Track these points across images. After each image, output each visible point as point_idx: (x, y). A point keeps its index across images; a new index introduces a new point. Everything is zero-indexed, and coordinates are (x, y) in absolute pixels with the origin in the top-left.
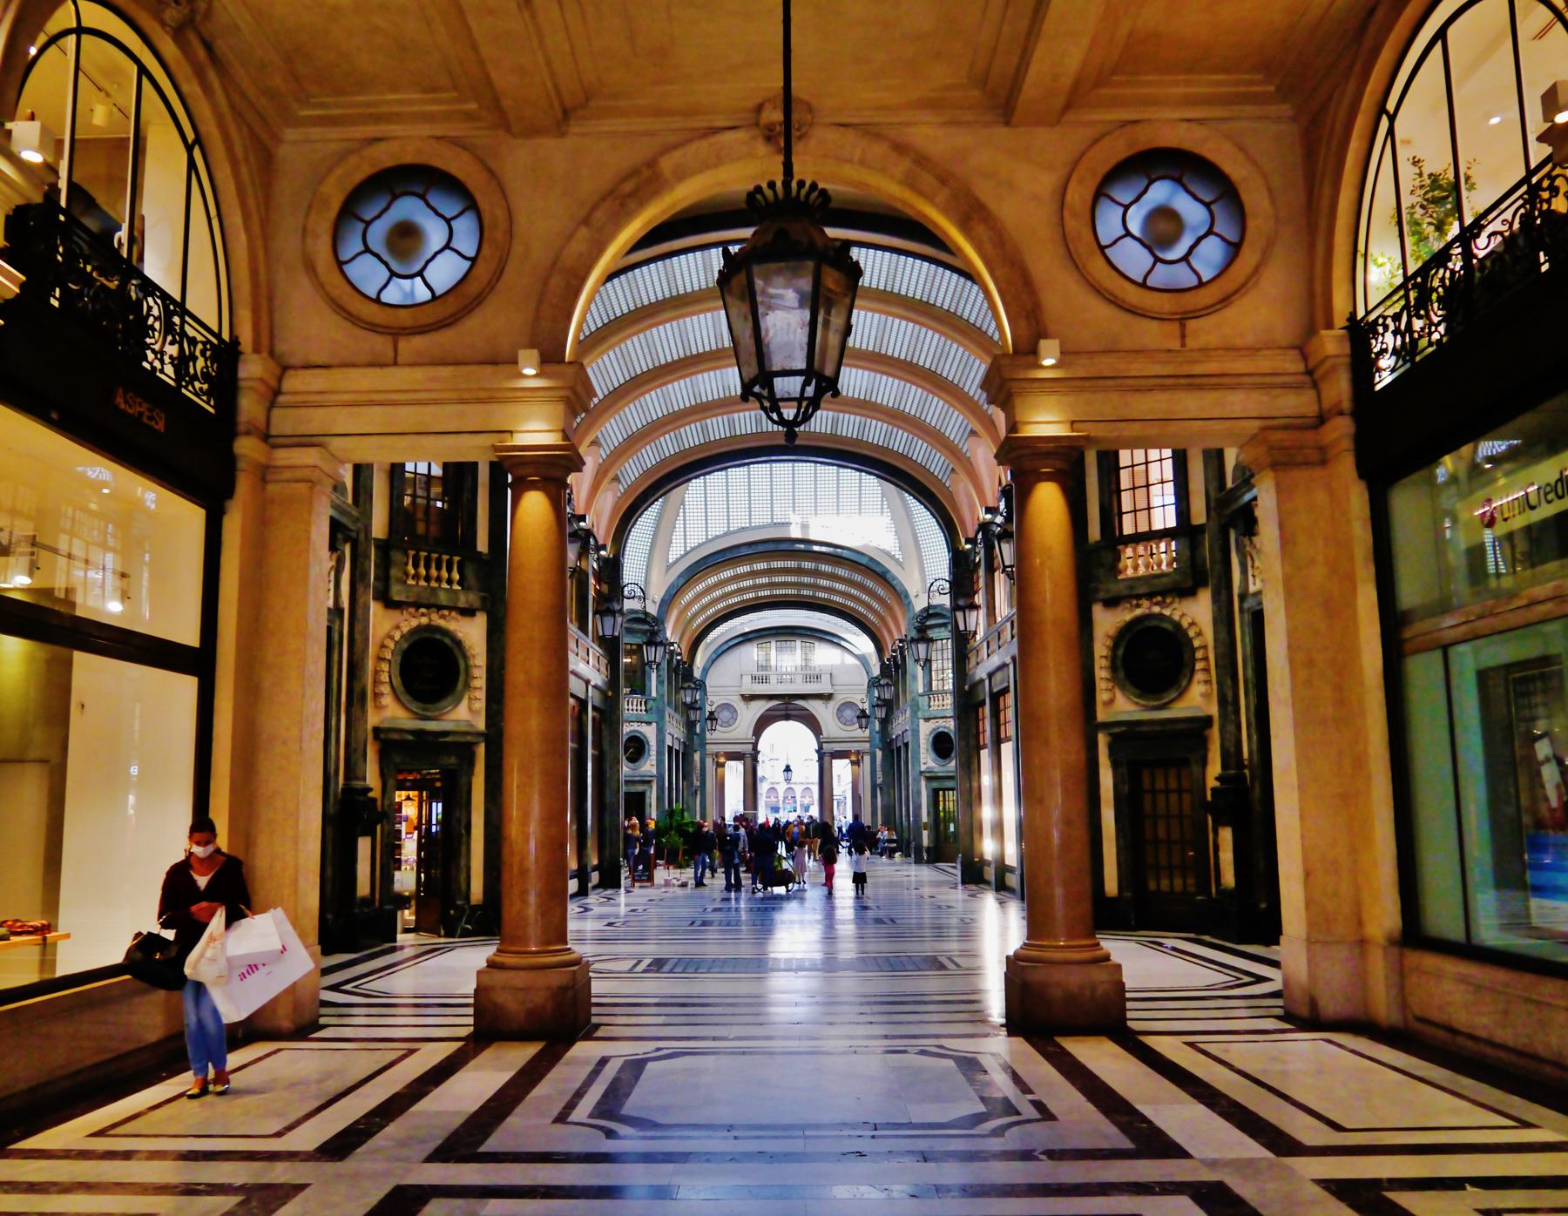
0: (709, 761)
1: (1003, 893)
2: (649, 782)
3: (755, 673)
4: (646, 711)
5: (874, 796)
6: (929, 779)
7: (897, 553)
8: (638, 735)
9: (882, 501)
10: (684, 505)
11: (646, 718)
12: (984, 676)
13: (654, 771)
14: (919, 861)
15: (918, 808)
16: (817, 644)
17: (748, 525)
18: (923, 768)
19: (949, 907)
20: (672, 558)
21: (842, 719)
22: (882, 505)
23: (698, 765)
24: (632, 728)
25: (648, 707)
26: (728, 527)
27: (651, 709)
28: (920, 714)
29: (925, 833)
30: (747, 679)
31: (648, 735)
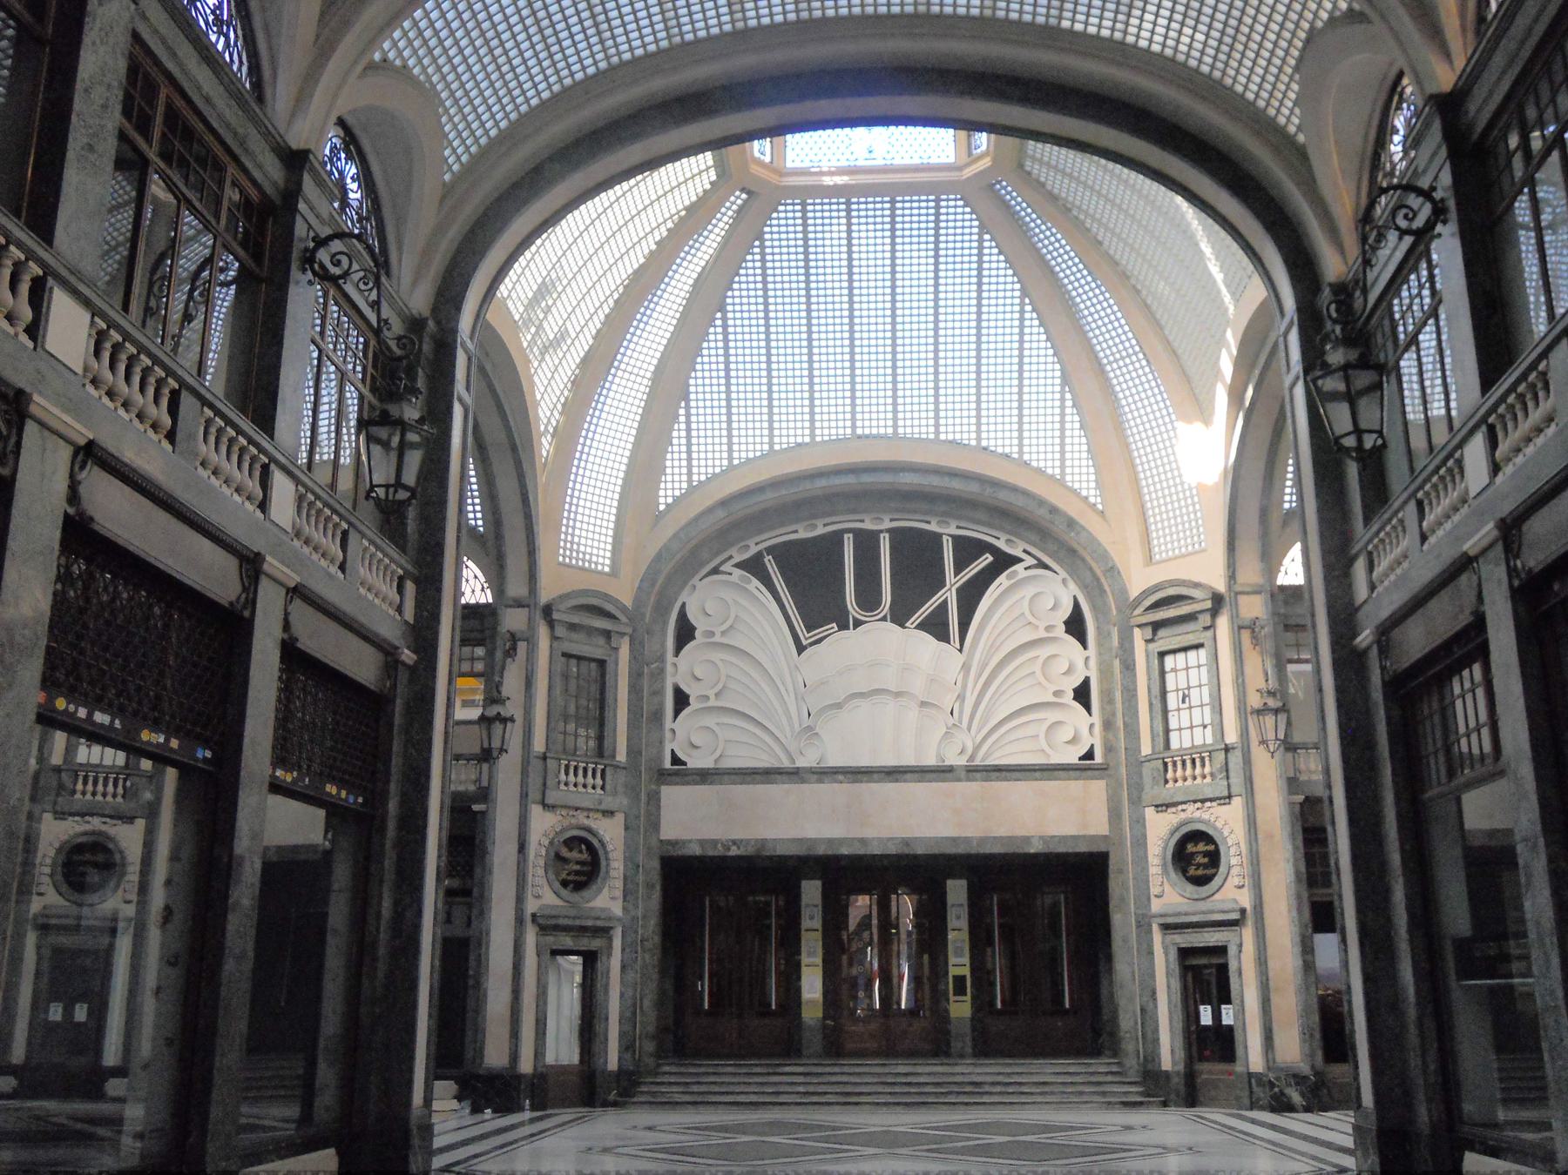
4: (603, 788)
7: (1092, 492)
9: (1062, 392)
10: (688, 401)
17: (807, 439)
18: (1156, 906)
20: (665, 497)
22: (1063, 400)
26: (771, 444)
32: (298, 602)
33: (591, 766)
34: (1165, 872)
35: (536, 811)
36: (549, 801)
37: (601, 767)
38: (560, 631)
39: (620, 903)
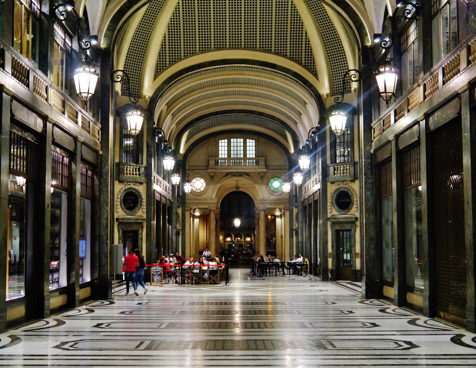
1: (381, 300)
2: (141, 223)
4: (139, 174)
5: (291, 237)
8: (134, 191)
12: (391, 137)
13: (145, 216)
14: (325, 279)
15: (325, 243)
18: (329, 215)
19: (351, 312)
23: (181, 216)
24: (129, 186)
29: (330, 260)
32: (14, 101)
33: (135, 167)
34: (332, 204)
35: (116, 183)
36: (121, 180)
37: (138, 167)
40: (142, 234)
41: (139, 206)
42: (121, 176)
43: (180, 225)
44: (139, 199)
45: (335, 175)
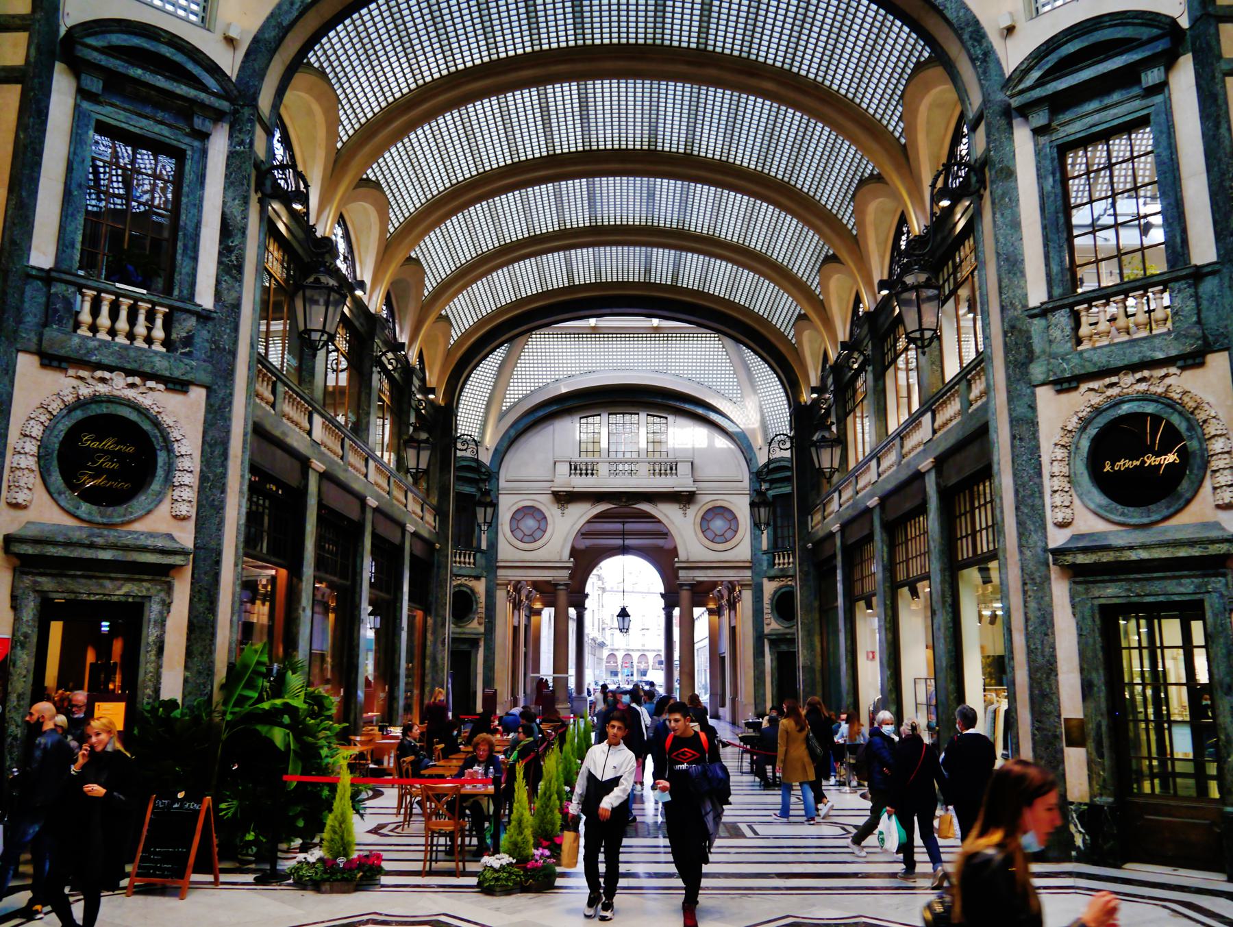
0: (501, 595)
3: (576, 458)
4: (167, 343)
5: (759, 653)
6: (1078, 574)
11: (161, 366)
13: (186, 537)
16: (671, 418)
18: (1057, 538)
21: (709, 533)
23: (482, 599)
24: (102, 389)
25: (178, 333)
27: (188, 341)
28: (1037, 371)
30: (563, 469)
31: (167, 420)
38: (95, 85)
39: (191, 525)
40: (162, 623)
41: (155, 486)
42: (52, 333)
43: (480, 624)
44: (162, 457)
45: (1085, 346)
